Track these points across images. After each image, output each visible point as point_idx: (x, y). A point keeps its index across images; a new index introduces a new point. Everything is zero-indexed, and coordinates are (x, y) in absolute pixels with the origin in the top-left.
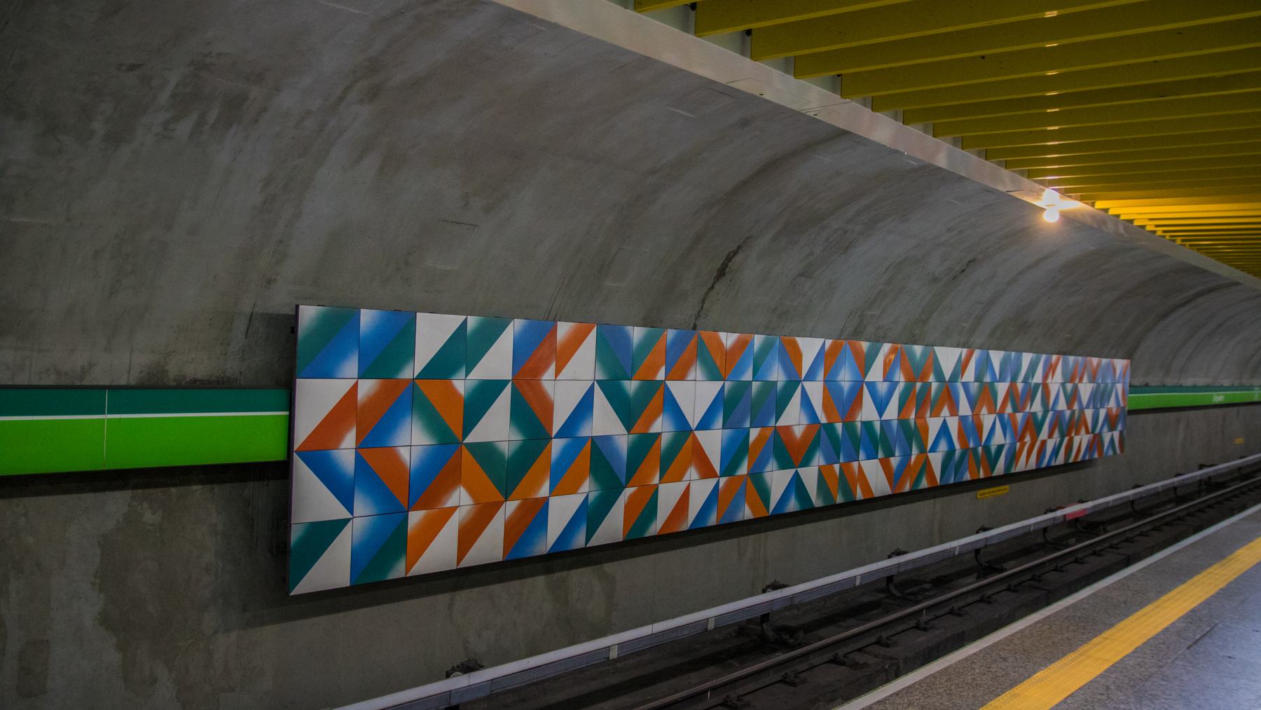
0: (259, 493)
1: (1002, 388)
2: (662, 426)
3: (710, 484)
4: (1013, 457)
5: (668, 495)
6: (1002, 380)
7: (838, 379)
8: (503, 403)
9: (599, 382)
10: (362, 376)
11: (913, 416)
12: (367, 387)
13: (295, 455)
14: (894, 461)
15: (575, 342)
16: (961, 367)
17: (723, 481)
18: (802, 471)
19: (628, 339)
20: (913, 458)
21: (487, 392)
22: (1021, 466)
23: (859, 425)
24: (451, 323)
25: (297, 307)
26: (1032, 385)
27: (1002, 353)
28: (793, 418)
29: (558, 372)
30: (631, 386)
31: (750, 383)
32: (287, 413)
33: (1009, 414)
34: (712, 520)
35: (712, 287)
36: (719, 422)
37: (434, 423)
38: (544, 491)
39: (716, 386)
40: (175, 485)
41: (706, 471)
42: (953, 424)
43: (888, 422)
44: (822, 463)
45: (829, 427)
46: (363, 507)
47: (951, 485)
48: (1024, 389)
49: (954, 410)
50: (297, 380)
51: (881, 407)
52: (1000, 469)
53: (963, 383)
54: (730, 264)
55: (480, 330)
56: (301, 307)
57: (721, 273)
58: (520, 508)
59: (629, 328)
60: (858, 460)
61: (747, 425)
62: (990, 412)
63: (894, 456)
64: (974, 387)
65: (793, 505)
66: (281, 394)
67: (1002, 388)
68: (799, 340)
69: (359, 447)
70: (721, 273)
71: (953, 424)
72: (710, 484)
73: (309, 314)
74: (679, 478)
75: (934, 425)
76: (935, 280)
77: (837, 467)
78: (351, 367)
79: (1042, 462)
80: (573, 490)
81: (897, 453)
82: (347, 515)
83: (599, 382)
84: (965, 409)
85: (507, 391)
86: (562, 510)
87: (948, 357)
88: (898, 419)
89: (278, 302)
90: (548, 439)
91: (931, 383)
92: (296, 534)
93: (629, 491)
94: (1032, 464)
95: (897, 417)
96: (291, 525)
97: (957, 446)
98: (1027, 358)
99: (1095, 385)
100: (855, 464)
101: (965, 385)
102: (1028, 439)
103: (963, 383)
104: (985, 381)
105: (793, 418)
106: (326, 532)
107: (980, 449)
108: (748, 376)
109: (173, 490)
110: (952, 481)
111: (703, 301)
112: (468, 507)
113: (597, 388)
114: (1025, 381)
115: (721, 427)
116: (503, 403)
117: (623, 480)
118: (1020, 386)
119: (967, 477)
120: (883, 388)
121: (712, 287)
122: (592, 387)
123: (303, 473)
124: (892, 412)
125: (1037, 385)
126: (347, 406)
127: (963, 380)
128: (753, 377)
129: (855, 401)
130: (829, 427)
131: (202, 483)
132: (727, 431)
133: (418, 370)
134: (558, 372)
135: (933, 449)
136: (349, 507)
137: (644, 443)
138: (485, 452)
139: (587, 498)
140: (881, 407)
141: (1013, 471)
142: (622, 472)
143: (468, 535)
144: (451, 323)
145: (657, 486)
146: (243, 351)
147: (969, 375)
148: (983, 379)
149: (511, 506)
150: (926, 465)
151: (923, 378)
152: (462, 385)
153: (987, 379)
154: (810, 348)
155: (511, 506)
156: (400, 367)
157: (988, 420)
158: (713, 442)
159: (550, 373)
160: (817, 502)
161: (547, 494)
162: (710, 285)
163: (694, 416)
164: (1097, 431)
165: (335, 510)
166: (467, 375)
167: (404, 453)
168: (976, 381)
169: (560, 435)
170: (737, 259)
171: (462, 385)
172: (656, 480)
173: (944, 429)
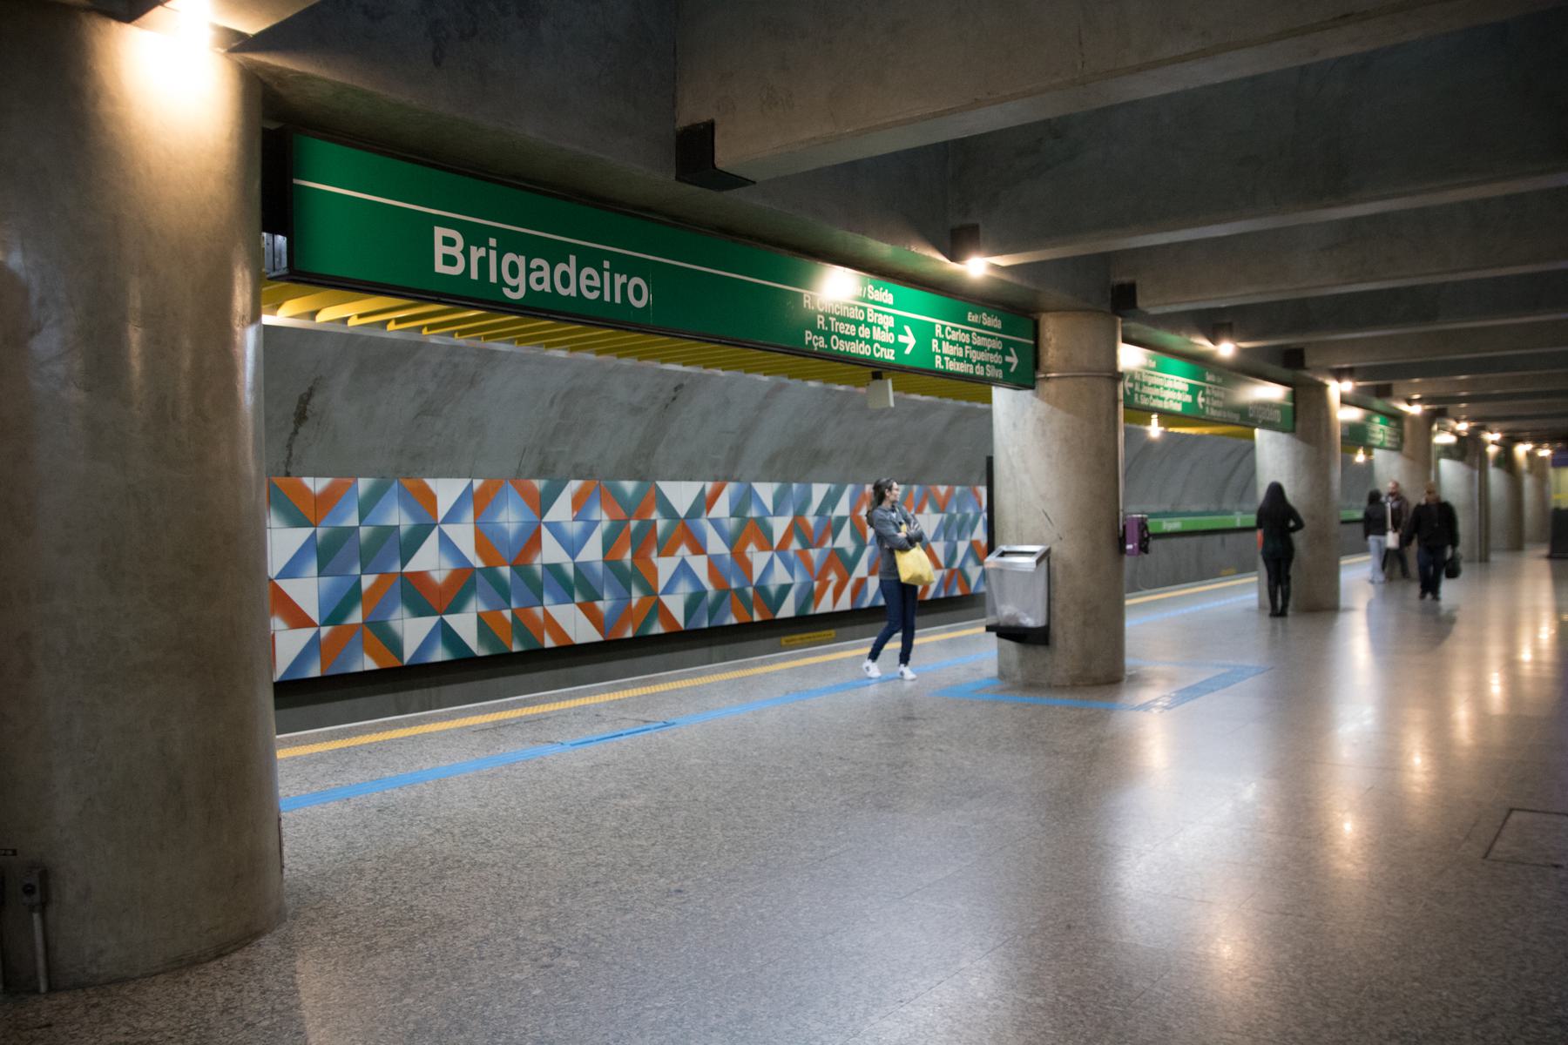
1: (780, 525)
3: (306, 634)
4: (810, 596)
6: (778, 510)
11: (628, 556)
14: (603, 606)
16: (705, 503)
17: (325, 631)
18: (453, 620)
20: (634, 602)
22: (825, 605)
23: (538, 569)
26: (833, 518)
27: (775, 486)
28: (429, 560)
31: (356, 528)
33: (796, 552)
34: (314, 671)
39: (303, 534)
42: (699, 565)
43: (587, 564)
44: (482, 608)
45: (490, 572)
47: (704, 630)
48: (817, 524)
49: (698, 548)
51: (573, 548)
52: (787, 610)
53: (710, 520)
54: (308, 407)
57: (301, 417)
60: (542, 605)
61: (357, 571)
62: (762, 548)
63: (601, 599)
64: (731, 524)
65: (440, 654)
67: (780, 525)
68: (431, 483)
70: (301, 417)
71: (699, 565)
75: (665, 567)
76: (636, 410)
77: (507, 614)
79: (862, 601)
81: (606, 596)
84: (716, 545)
87: (681, 495)
88: (604, 561)
91: (655, 521)
94: (845, 603)
97: (709, 587)
98: (819, 491)
99: (945, 516)
100: (538, 611)
101: (716, 523)
102: (833, 577)
103: (710, 520)
104: (749, 515)
105: (429, 560)
107: (750, 590)
108: (352, 520)
110: (705, 625)
111: (289, 447)
114: (820, 512)
115: (316, 575)
118: (811, 519)
119: (732, 620)
120: (574, 528)
121: (296, 432)
124: (592, 552)
125: (841, 520)
127: (711, 516)
129: (535, 542)
130: (490, 572)
132: (326, 580)
135: (669, 589)
140: (573, 548)
141: (811, 612)
147: (722, 508)
148: (745, 513)
150: (660, 610)
151: (642, 513)
153: (753, 513)
154: (447, 491)
157: (758, 559)
160: (478, 650)
162: (292, 430)
164: (956, 565)
168: (732, 516)
170: (317, 401)
173: (684, 569)
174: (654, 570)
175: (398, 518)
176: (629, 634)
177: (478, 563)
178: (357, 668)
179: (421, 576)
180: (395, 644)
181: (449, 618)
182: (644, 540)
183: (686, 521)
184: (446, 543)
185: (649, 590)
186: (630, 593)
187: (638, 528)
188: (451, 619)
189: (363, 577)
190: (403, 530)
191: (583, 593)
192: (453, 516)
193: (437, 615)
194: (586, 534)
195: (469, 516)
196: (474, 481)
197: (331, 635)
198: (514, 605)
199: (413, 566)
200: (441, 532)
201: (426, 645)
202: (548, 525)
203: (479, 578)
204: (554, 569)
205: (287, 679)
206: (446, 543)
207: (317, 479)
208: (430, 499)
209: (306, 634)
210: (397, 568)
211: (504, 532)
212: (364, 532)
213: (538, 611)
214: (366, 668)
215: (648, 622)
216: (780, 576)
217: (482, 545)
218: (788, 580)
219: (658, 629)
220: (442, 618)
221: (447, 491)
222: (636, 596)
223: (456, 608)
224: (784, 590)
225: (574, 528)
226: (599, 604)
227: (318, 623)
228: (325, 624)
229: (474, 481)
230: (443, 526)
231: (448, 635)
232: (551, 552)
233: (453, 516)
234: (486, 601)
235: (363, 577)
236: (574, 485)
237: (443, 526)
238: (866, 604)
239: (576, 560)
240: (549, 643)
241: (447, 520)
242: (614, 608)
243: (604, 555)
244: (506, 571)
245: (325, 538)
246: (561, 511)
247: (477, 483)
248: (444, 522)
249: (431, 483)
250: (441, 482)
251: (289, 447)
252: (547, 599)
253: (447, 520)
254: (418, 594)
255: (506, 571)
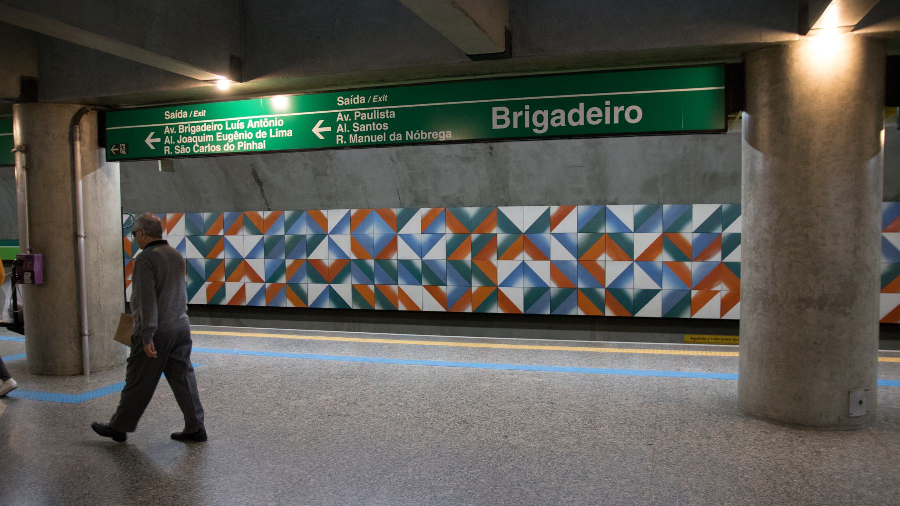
2: (225, 256)
3: (260, 285)
5: (232, 289)
7: (453, 235)
11: (468, 258)
14: (447, 289)
15: (175, 221)
16: (546, 222)
19: (201, 218)
23: (395, 263)
28: (322, 253)
30: (205, 238)
31: (283, 236)
34: (263, 303)
35: (262, 190)
36: (263, 254)
39: (258, 238)
41: (256, 278)
44: (355, 282)
51: (422, 251)
52: (653, 309)
53: (555, 235)
60: (397, 284)
61: (284, 257)
65: (328, 304)
68: (324, 212)
72: (258, 286)
74: (238, 280)
81: (449, 283)
83: (188, 236)
91: (496, 235)
95: (446, 258)
97: (554, 286)
100: (395, 288)
103: (555, 235)
105: (322, 253)
108: (282, 232)
111: (264, 196)
117: (204, 278)
120: (423, 238)
121: (262, 190)
122: (185, 239)
124: (438, 253)
128: (285, 233)
130: (361, 263)
132: (268, 261)
137: (214, 265)
141: (687, 315)
142: (204, 275)
145: (224, 284)
150: (498, 296)
158: (260, 265)
163: (244, 252)
168: (580, 231)
170: (260, 175)
172: (224, 280)
174: (495, 269)
175: (305, 230)
176: (469, 310)
177: (353, 257)
178: (283, 305)
179: (318, 262)
180: (304, 296)
181: (334, 286)
182: (485, 246)
183: (527, 235)
184: (333, 245)
185: (489, 281)
186: (471, 283)
187: (478, 240)
188: (336, 287)
189: (286, 260)
190: (308, 237)
191: (428, 279)
192: (338, 230)
193: (328, 283)
194: (433, 243)
195: (348, 230)
196: (352, 210)
197: (270, 287)
198: (376, 282)
199: (314, 256)
200: (330, 239)
201: (321, 298)
202: (403, 236)
203: (354, 265)
204: (407, 264)
206: (333, 245)
207: (265, 212)
208: (325, 221)
209: (260, 285)
210: (304, 257)
211: (372, 240)
212: (287, 238)
213: (395, 288)
214: (288, 306)
215: (488, 302)
216: (641, 280)
217: (354, 247)
218: (654, 286)
219: (496, 309)
220: (329, 285)
221: (334, 217)
222: (476, 285)
223: (339, 280)
224: (646, 296)
225: (423, 238)
226: (443, 288)
227: (265, 281)
228: (268, 282)
229: (352, 210)
230: (331, 236)
231: (335, 296)
232: (404, 252)
233: (338, 230)
234: (356, 277)
235: (286, 260)
236: (424, 211)
237: (331, 236)
238: (226, 301)
239: (423, 259)
240: (402, 307)
241: (334, 232)
242: (453, 293)
243: (447, 257)
244: (371, 262)
245: (268, 241)
246: (413, 227)
247: (353, 212)
248: (331, 234)
249: (324, 212)
250: (331, 211)
251: (264, 196)
252: (401, 281)
253: (334, 232)
254: (316, 272)
255: (371, 262)
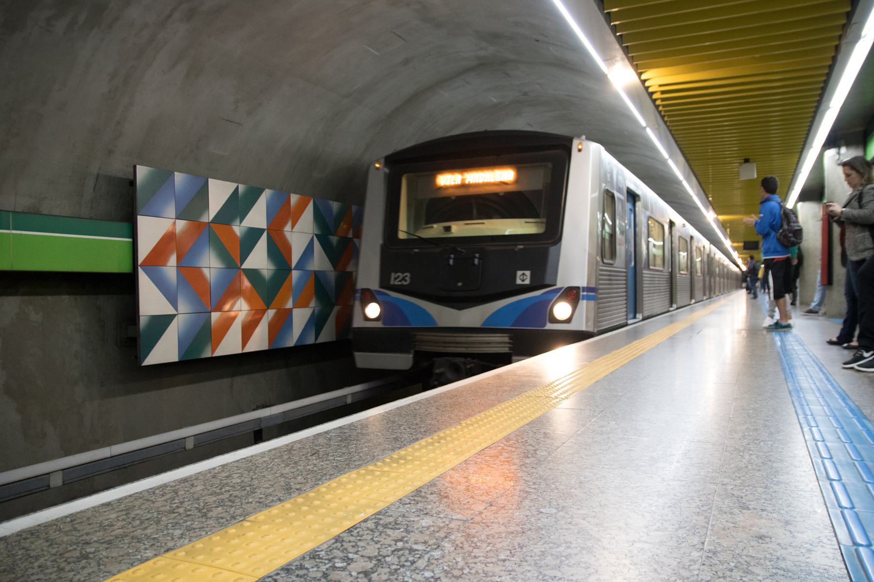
0: (108, 304)
8: (262, 243)
9: (316, 235)
10: (178, 217)
12: (181, 225)
13: (140, 269)
21: (253, 235)
24: (229, 187)
25: (135, 167)
29: (293, 227)
32: (130, 240)
37: (224, 255)
38: (289, 305)
40: (50, 294)
46: (183, 307)
50: (138, 216)
55: (245, 194)
56: (138, 166)
58: (276, 314)
59: (331, 202)
66: (125, 226)
69: (179, 267)
73: (142, 172)
78: (171, 210)
80: (306, 306)
82: (173, 312)
83: (316, 235)
85: (264, 237)
86: (300, 317)
89: (117, 167)
90: (290, 270)
92: (143, 321)
93: (336, 309)
96: (139, 316)
106: (161, 323)
109: (49, 298)
112: (246, 312)
113: (315, 239)
116: (262, 243)
123: (144, 281)
126: (168, 241)
131: (69, 294)
133: (211, 218)
134: (293, 227)
136: (175, 305)
138: (253, 275)
139: (314, 311)
143: (248, 331)
144: (229, 187)
146: (92, 202)
149: (271, 313)
152: (238, 229)
155: (271, 313)
156: (200, 214)
159: (288, 228)
161: (291, 307)
165: (165, 308)
166: (241, 222)
167: (206, 272)
169: (296, 268)
171: (238, 229)
205: (184, 359)
